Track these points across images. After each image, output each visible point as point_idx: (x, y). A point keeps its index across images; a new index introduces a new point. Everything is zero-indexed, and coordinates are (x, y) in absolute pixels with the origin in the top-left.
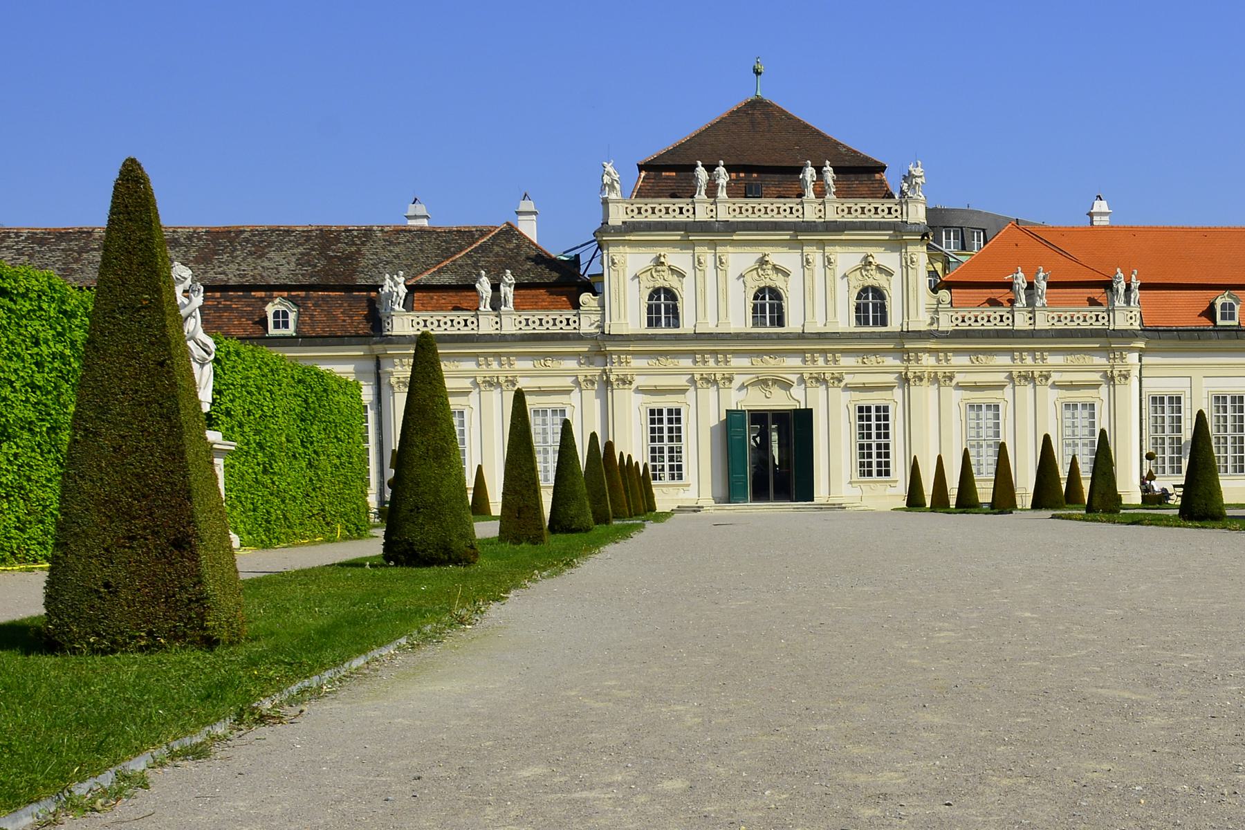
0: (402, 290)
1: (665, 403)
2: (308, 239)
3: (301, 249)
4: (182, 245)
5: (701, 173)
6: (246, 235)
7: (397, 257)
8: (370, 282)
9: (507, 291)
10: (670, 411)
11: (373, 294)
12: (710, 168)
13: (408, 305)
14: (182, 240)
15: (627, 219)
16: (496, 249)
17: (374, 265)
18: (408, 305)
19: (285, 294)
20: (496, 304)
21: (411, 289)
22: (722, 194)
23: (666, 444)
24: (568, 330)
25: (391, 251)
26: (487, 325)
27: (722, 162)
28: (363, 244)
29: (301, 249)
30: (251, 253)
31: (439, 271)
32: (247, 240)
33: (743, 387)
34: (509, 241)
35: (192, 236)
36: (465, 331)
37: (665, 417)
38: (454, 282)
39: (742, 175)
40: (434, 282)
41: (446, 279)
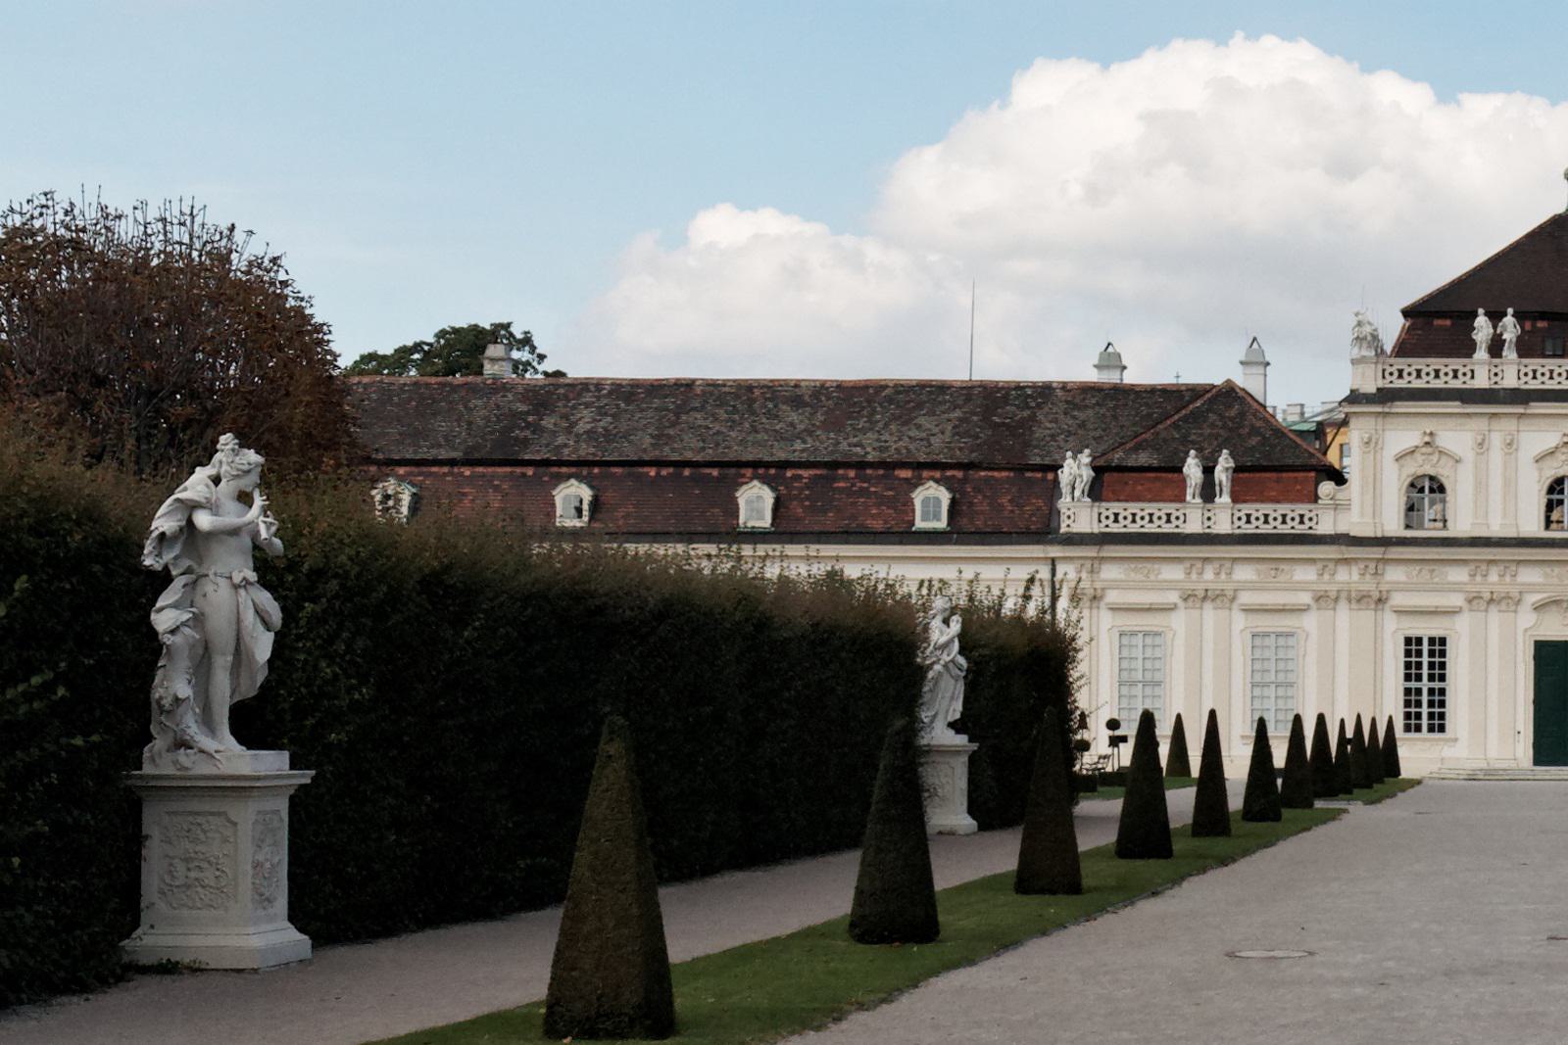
0: (1087, 474)
1: (1426, 629)
2: (968, 398)
3: (958, 413)
4: (807, 405)
5: (1482, 321)
6: (887, 392)
7: (1082, 425)
8: (1047, 461)
9: (1221, 474)
10: (1432, 641)
11: (1050, 476)
12: (1495, 317)
13: (1096, 492)
14: (807, 398)
15: (1381, 384)
16: (1212, 417)
17: (1053, 437)
18: (1096, 492)
19: (938, 474)
20: (1208, 492)
21: (1098, 470)
22: (1510, 354)
23: (1425, 685)
24: (1300, 529)
25: (1074, 418)
26: (1194, 526)
27: (1510, 311)
28: (1039, 406)
29: (958, 413)
30: (895, 418)
31: (1136, 449)
32: (890, 400)
33: (1539, 608)
34: (1230, 407)
35: (819, 392)
36: (1168, 529)
37: (1425, 647)
38: (1155, 463)
39: (1540, 324)
40: (1131, 463)
41: (1143, 458)
